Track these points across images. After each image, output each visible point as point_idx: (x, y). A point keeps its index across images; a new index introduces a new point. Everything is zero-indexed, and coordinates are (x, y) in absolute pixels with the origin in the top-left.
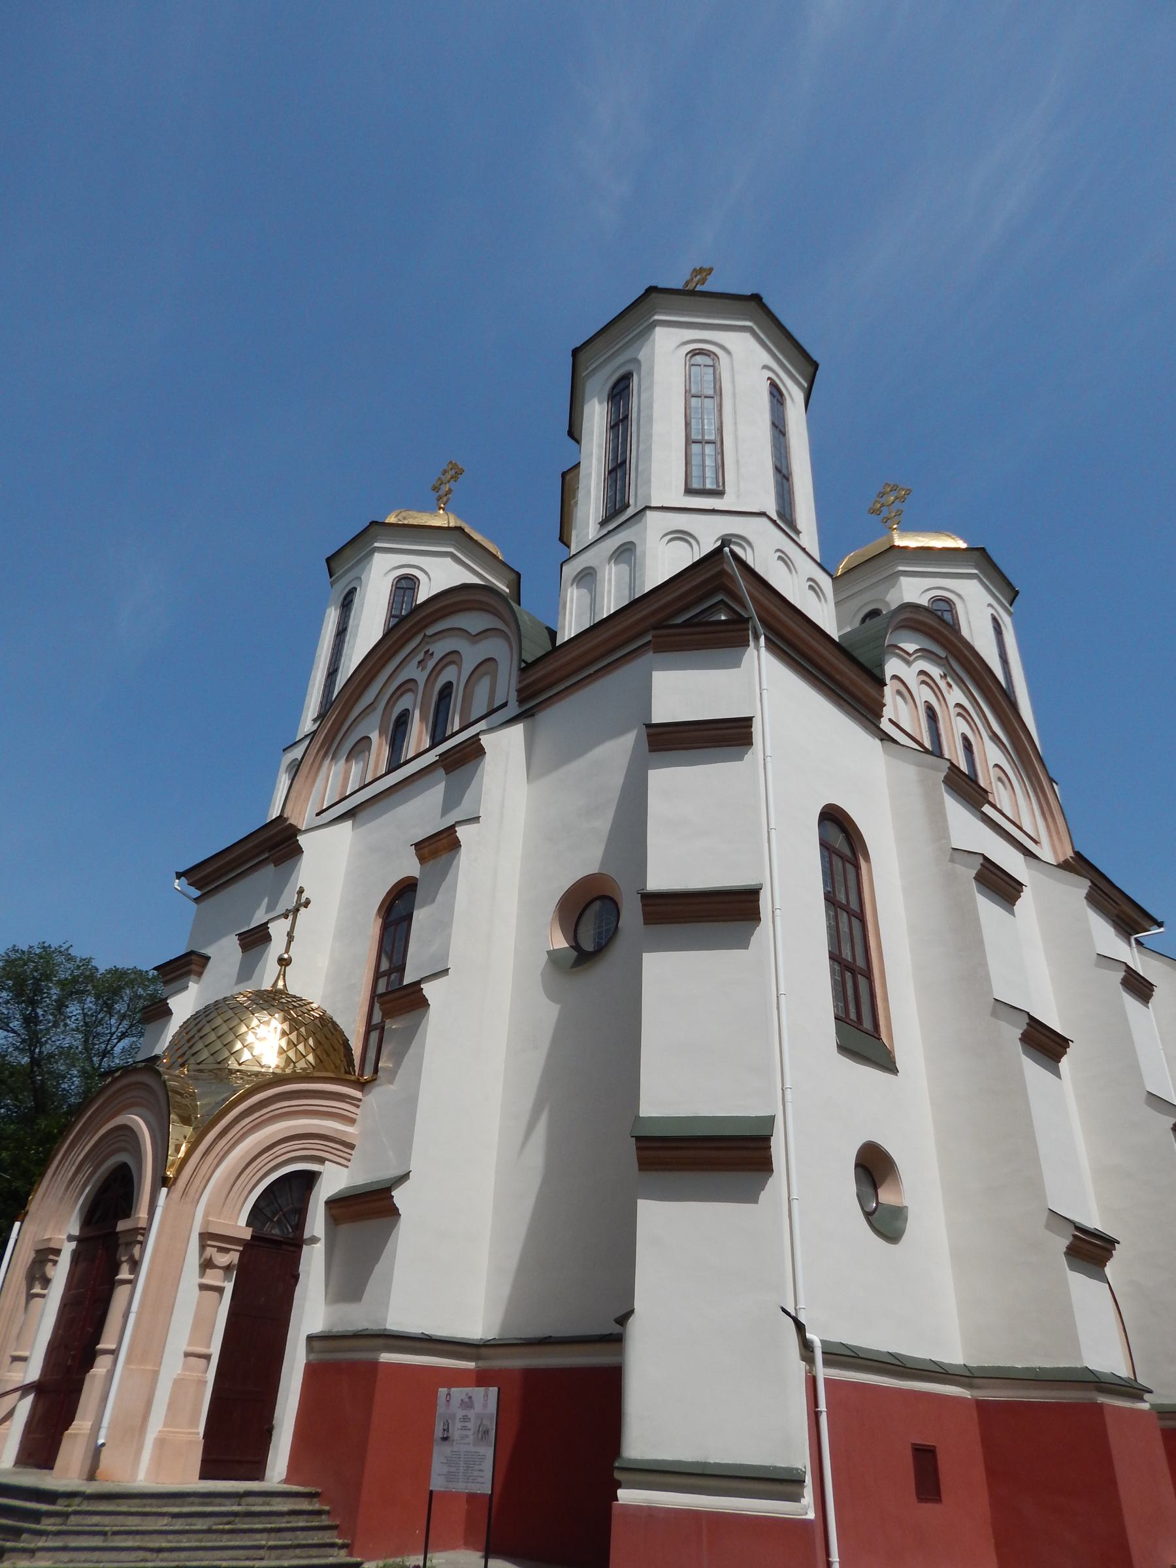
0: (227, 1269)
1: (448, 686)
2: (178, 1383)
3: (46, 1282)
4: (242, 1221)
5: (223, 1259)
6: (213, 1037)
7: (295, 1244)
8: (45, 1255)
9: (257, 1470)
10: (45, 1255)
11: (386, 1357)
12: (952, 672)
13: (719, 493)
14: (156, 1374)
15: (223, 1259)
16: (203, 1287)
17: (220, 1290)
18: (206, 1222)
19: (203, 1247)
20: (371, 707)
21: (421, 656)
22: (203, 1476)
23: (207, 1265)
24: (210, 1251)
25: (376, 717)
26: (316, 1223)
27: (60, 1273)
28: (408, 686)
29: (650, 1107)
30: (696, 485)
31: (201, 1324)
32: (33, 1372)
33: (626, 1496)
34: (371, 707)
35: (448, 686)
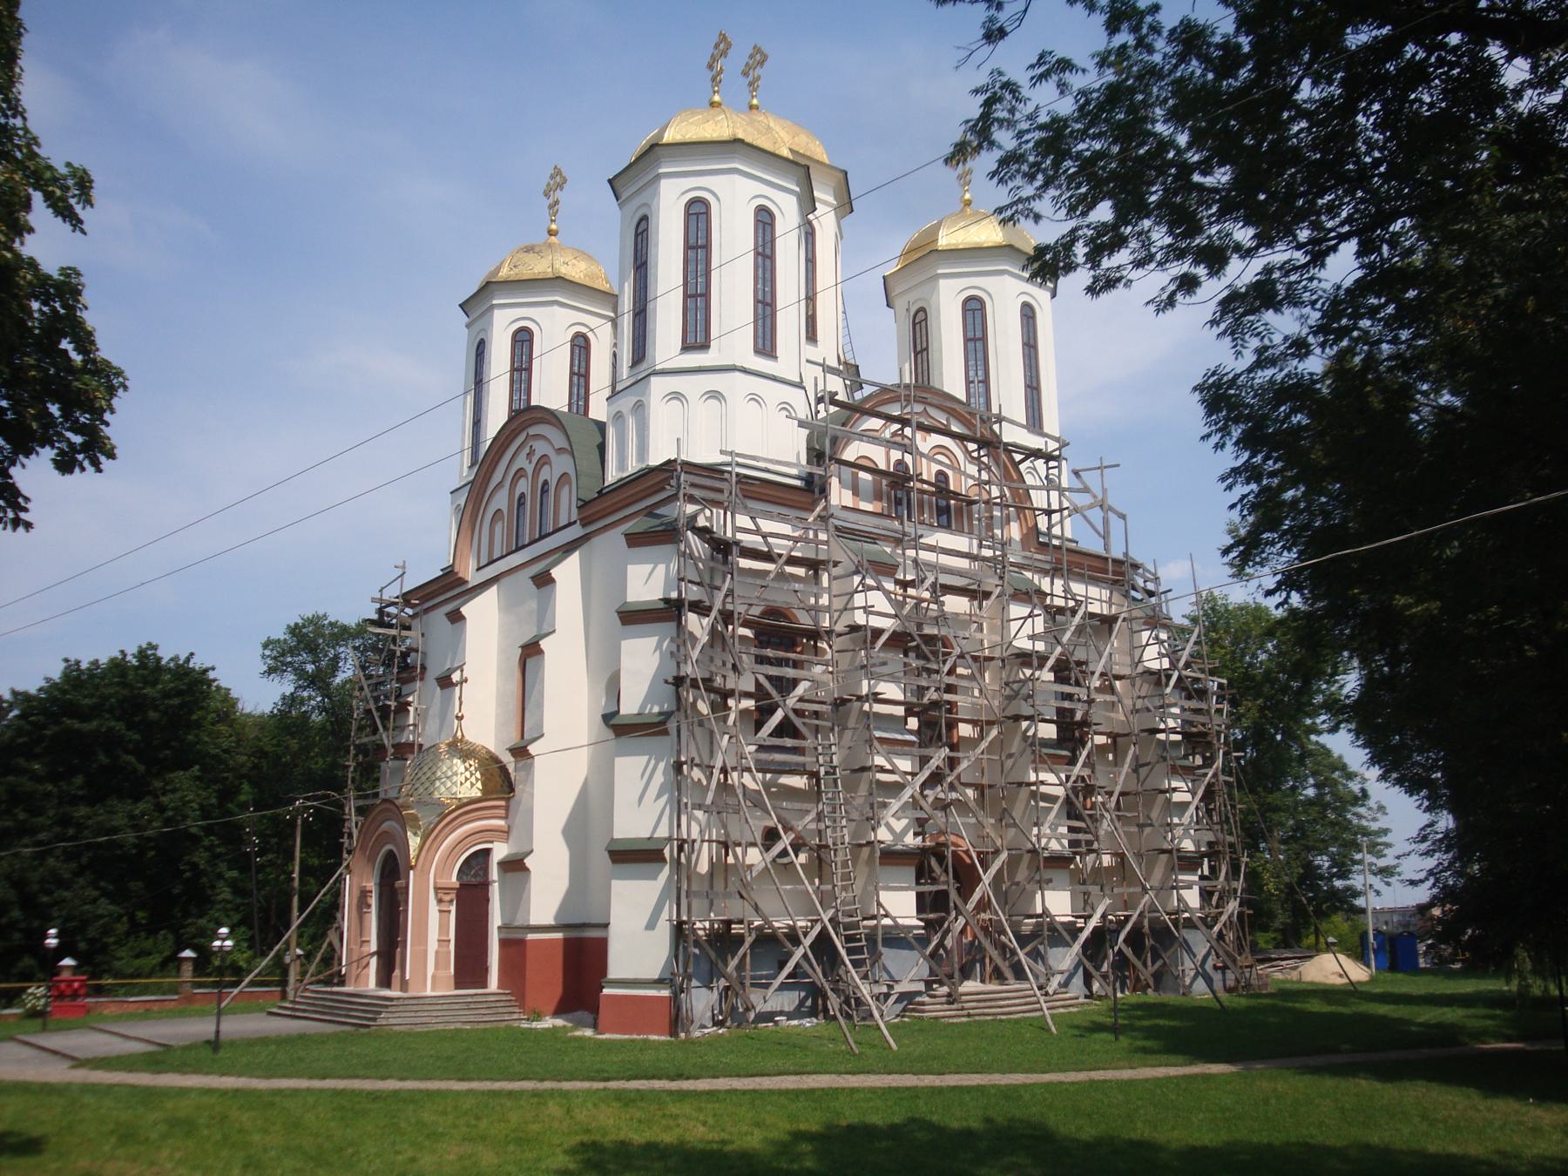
0: (451, 901)
1: (546, 483)
2: (437, 953)
3: (369, 906)
4: (454, 878)
5: (447, 898)
6: (424, 779)
7: (485, 885)
8: (364, 894)
9: (485, 985)
10: (364, 894)
11: (530, 936)
13: (705, 346)
14: (426, 951)
15: (447, 898)
16: (440, 911)
17: (449, 912)
18: (435, 883)
19: (436, 893)
20: (500, 484)
21: (527, 450)
22: (456, 988)
23: (440, 901)
24: (440, 895)
25: (504, 492)
26: (494, 873)
27: (373, 901)
28: (520, 473)
29: (617, 835)
30: (691, 340)
31: (443, 927)
32: (374, 947)
33: (606, 991)
34: (500, 484)
35: (546, 483)
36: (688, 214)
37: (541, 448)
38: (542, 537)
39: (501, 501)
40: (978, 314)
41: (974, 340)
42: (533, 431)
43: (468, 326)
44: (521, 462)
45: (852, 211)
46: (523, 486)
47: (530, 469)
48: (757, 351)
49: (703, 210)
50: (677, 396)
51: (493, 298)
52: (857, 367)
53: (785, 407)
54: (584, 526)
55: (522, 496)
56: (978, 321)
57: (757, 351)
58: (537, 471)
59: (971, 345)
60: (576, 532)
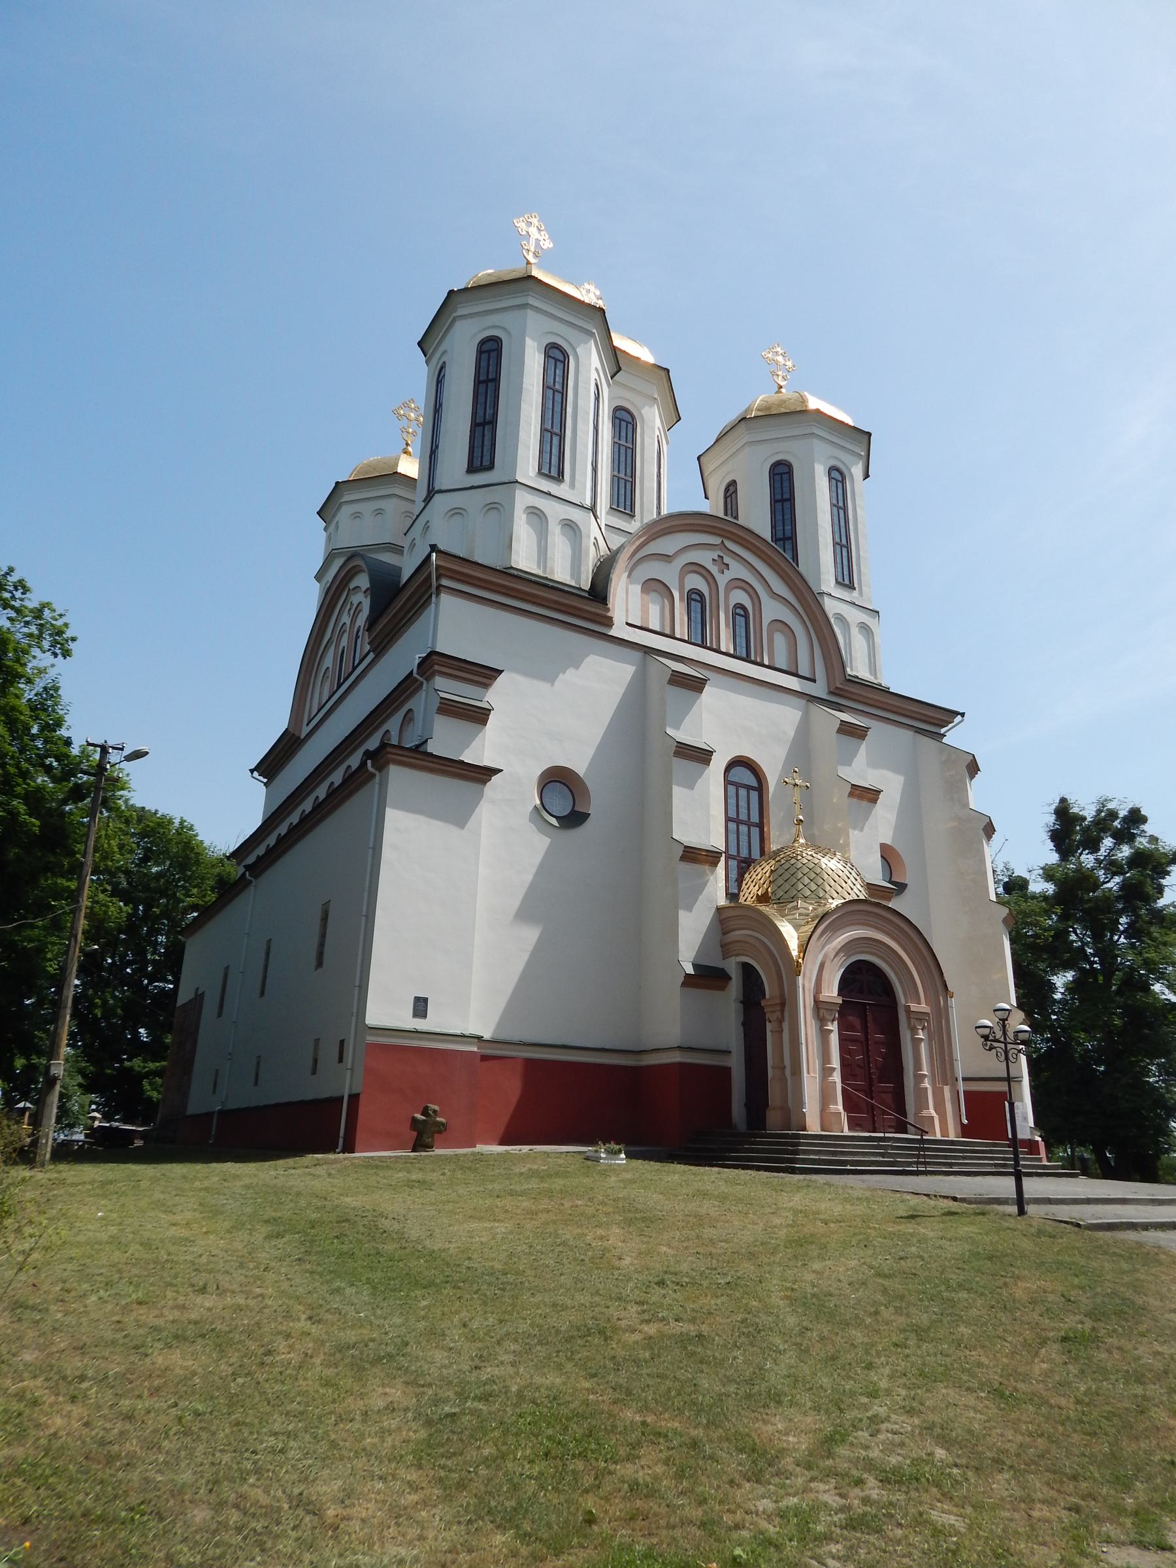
12: (727, 552)
36: (480, 352)
37: (357, 598)
40: (785, 477)
41: (783, 501)
42: (352, 585)
43: (325, 529)
44: (346, 619)
46: (344, 642)
49: (495, 346)
50: (457, 512)
51: (342, 496)
56: (786, 484)
59: (779, 505)
60: (372, 656)
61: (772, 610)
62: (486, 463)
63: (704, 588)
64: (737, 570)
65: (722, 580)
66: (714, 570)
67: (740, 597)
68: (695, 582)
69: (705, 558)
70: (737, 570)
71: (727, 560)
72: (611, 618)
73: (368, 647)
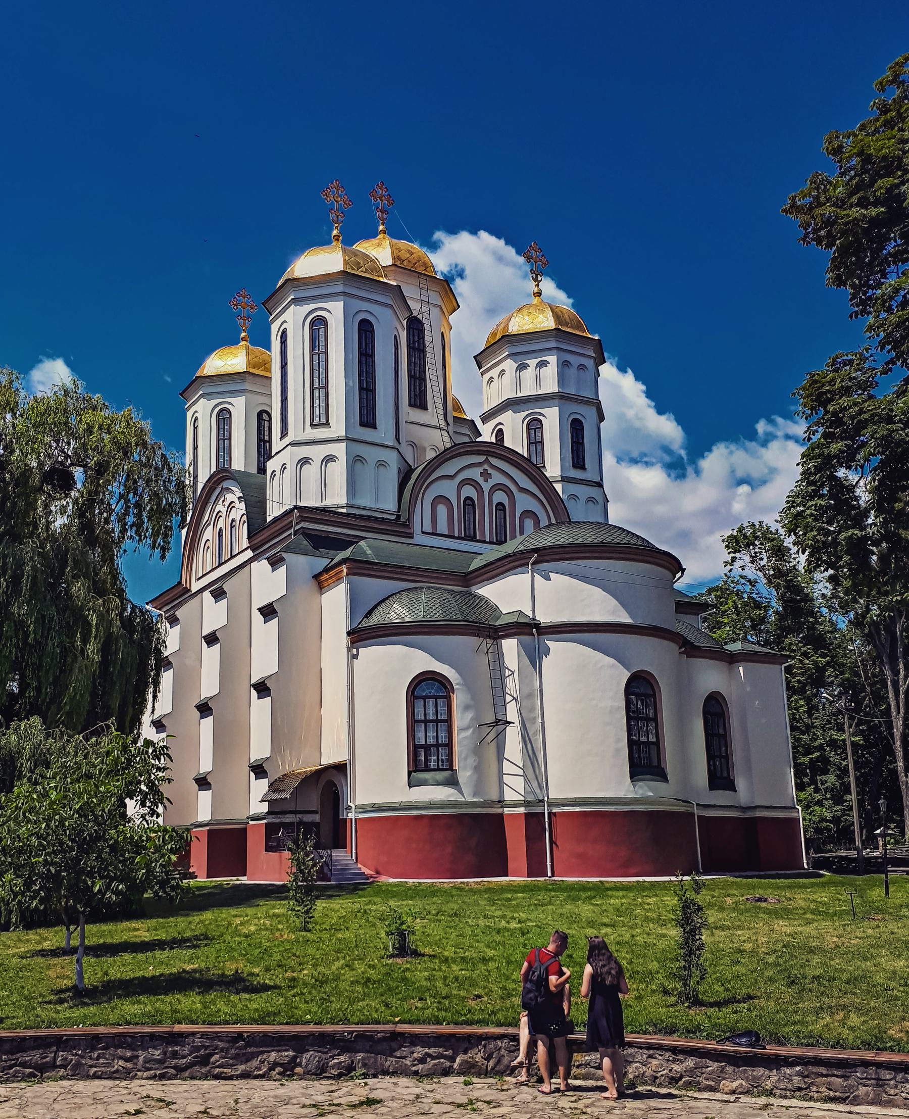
13: (327, 424)
21: (223, 499)
37: (230, 497)
38: (232, 557)
39: (208, 534)
42: (225, 484)
44: (219, 507)
45: (459, 306)
46: (221, 523)
47: (224, 510)
48: (362, 424)
52: (473, 421)
53: (381, 464)
54: (253, 551)
55: (221, 530)
57: (362, 424)
58: (228, 512)
60: (249, 554)
61: (524, 503)
62: (323, 420)
63: (475, 496)
64: (497, 478)
65: (486, 487)
66: (481, 480)
67: (500, 497)
68: (469, 491)
69: (474, 474)
70: (497, 478)
71: (490, 471)
72: (412, 534)
73: (245, 546)
